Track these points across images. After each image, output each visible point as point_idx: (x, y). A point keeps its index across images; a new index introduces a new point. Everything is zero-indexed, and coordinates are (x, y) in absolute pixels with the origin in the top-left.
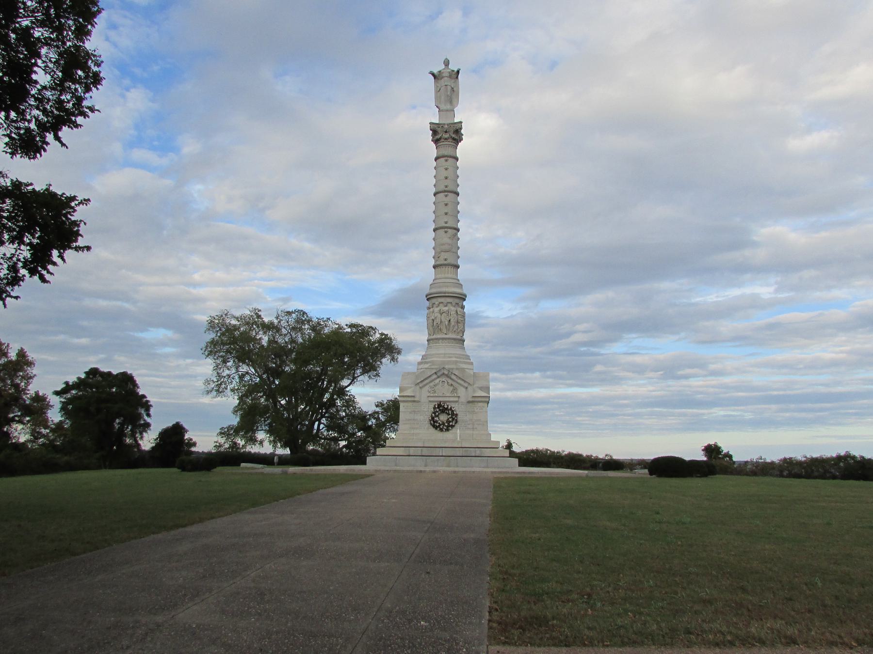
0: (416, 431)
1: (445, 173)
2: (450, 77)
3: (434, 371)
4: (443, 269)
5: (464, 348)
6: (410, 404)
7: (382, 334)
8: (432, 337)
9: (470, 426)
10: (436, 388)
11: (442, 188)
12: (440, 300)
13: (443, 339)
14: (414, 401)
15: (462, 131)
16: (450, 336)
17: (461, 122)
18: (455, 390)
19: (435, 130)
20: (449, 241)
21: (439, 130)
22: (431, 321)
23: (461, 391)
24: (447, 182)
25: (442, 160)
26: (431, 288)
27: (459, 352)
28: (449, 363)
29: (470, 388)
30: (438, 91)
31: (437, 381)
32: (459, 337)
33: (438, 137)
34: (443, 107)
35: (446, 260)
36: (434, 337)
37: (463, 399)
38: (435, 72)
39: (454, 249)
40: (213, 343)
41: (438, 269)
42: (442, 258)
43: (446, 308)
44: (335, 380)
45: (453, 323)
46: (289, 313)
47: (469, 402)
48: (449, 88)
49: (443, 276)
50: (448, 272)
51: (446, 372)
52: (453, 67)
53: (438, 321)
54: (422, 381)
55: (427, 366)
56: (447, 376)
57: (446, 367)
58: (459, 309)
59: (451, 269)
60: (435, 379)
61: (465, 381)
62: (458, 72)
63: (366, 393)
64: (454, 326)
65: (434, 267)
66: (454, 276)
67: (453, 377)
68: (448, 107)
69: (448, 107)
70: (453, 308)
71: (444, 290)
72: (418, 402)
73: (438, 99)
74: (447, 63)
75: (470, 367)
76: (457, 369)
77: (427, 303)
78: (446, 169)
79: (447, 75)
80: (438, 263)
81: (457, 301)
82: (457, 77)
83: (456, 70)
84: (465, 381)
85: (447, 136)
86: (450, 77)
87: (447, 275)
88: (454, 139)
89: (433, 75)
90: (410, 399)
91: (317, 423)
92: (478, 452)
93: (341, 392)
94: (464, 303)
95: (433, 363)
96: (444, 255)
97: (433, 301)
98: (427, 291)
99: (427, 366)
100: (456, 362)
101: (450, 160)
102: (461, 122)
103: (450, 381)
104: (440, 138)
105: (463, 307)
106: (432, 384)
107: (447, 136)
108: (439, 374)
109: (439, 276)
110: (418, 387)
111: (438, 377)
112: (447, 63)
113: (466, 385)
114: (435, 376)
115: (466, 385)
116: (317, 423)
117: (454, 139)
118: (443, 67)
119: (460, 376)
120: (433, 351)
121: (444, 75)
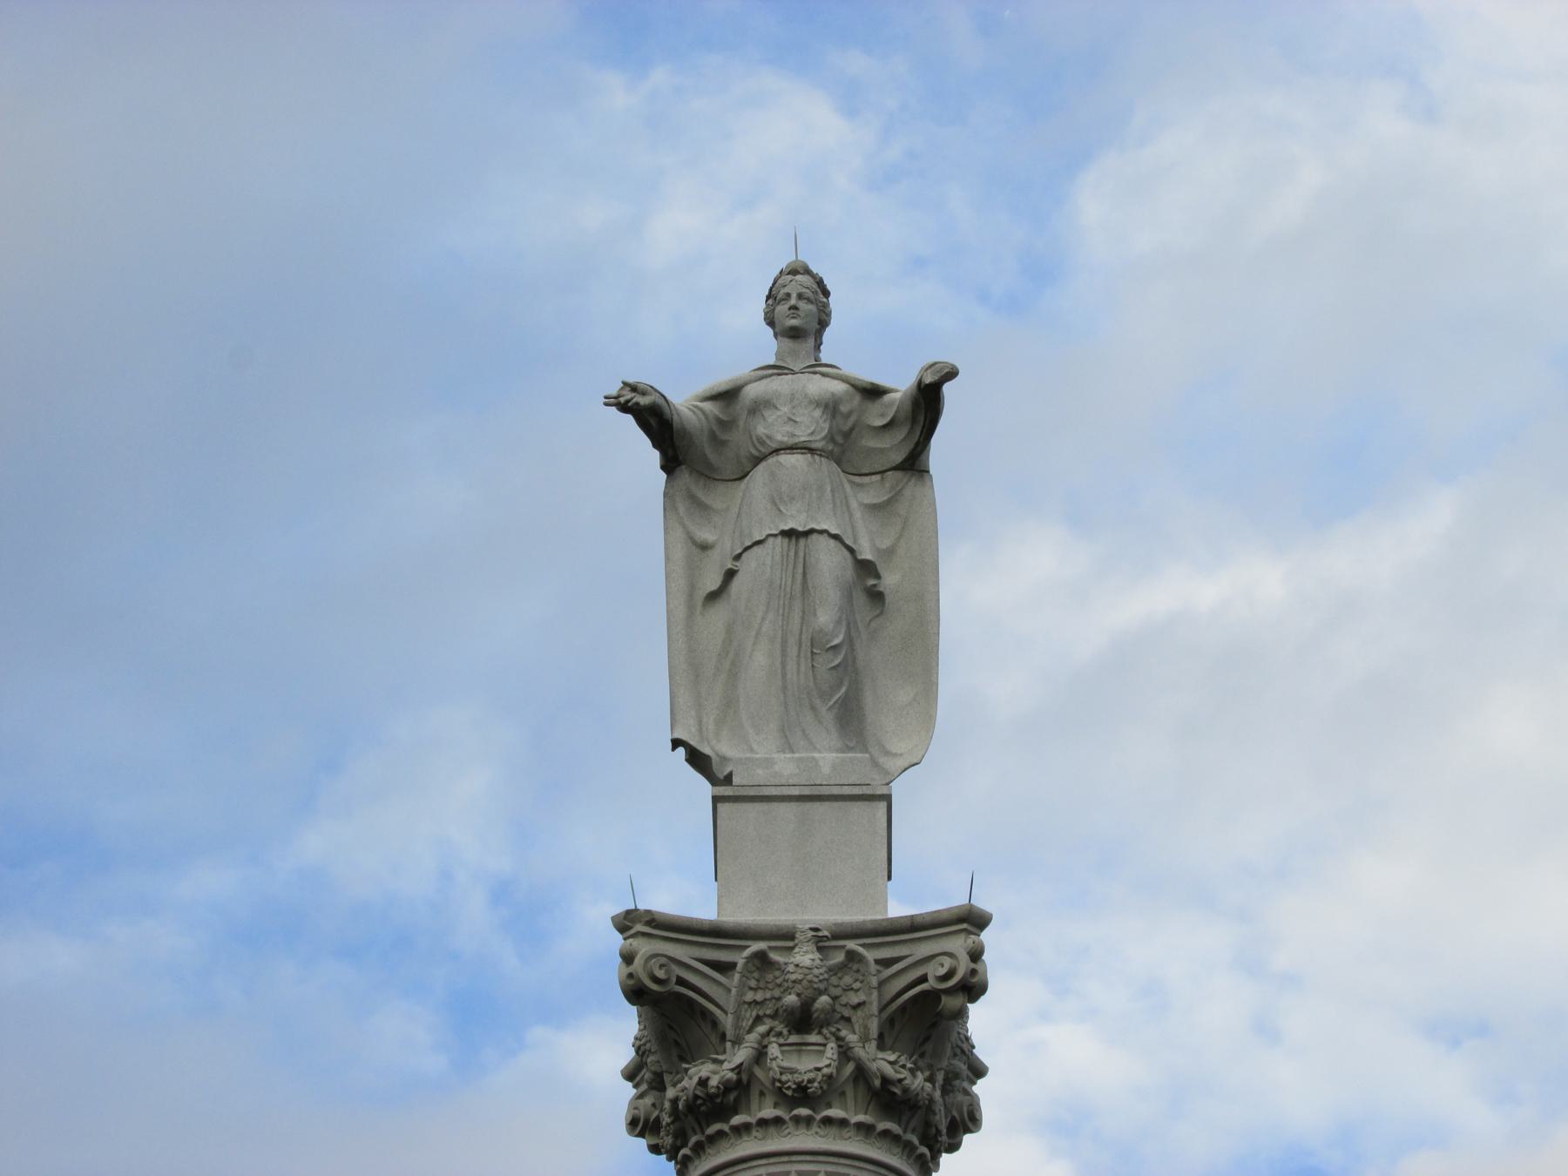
17: (974, 920)
19: (677, 995)
21: (726, 997)
30: (707, 591)
33: (712, 1072)
34: (761, 756)
38: (682, 395)
48: (828, 562)
62: (927, 401)
68: (827, 760)
69: (827, 760)
73: (700, 672)
79: (810, 427)
82: (914, 464)
83: (901, 382)
85: (812, 1062)
88: (888, 1099)
89: (654, 419)
102: (974, 920)
104: (740, 1089)
107: (812, 1062)
112: (799, 309)
117: (888, 1099)
118: (765, 346)
121: (773, 427)
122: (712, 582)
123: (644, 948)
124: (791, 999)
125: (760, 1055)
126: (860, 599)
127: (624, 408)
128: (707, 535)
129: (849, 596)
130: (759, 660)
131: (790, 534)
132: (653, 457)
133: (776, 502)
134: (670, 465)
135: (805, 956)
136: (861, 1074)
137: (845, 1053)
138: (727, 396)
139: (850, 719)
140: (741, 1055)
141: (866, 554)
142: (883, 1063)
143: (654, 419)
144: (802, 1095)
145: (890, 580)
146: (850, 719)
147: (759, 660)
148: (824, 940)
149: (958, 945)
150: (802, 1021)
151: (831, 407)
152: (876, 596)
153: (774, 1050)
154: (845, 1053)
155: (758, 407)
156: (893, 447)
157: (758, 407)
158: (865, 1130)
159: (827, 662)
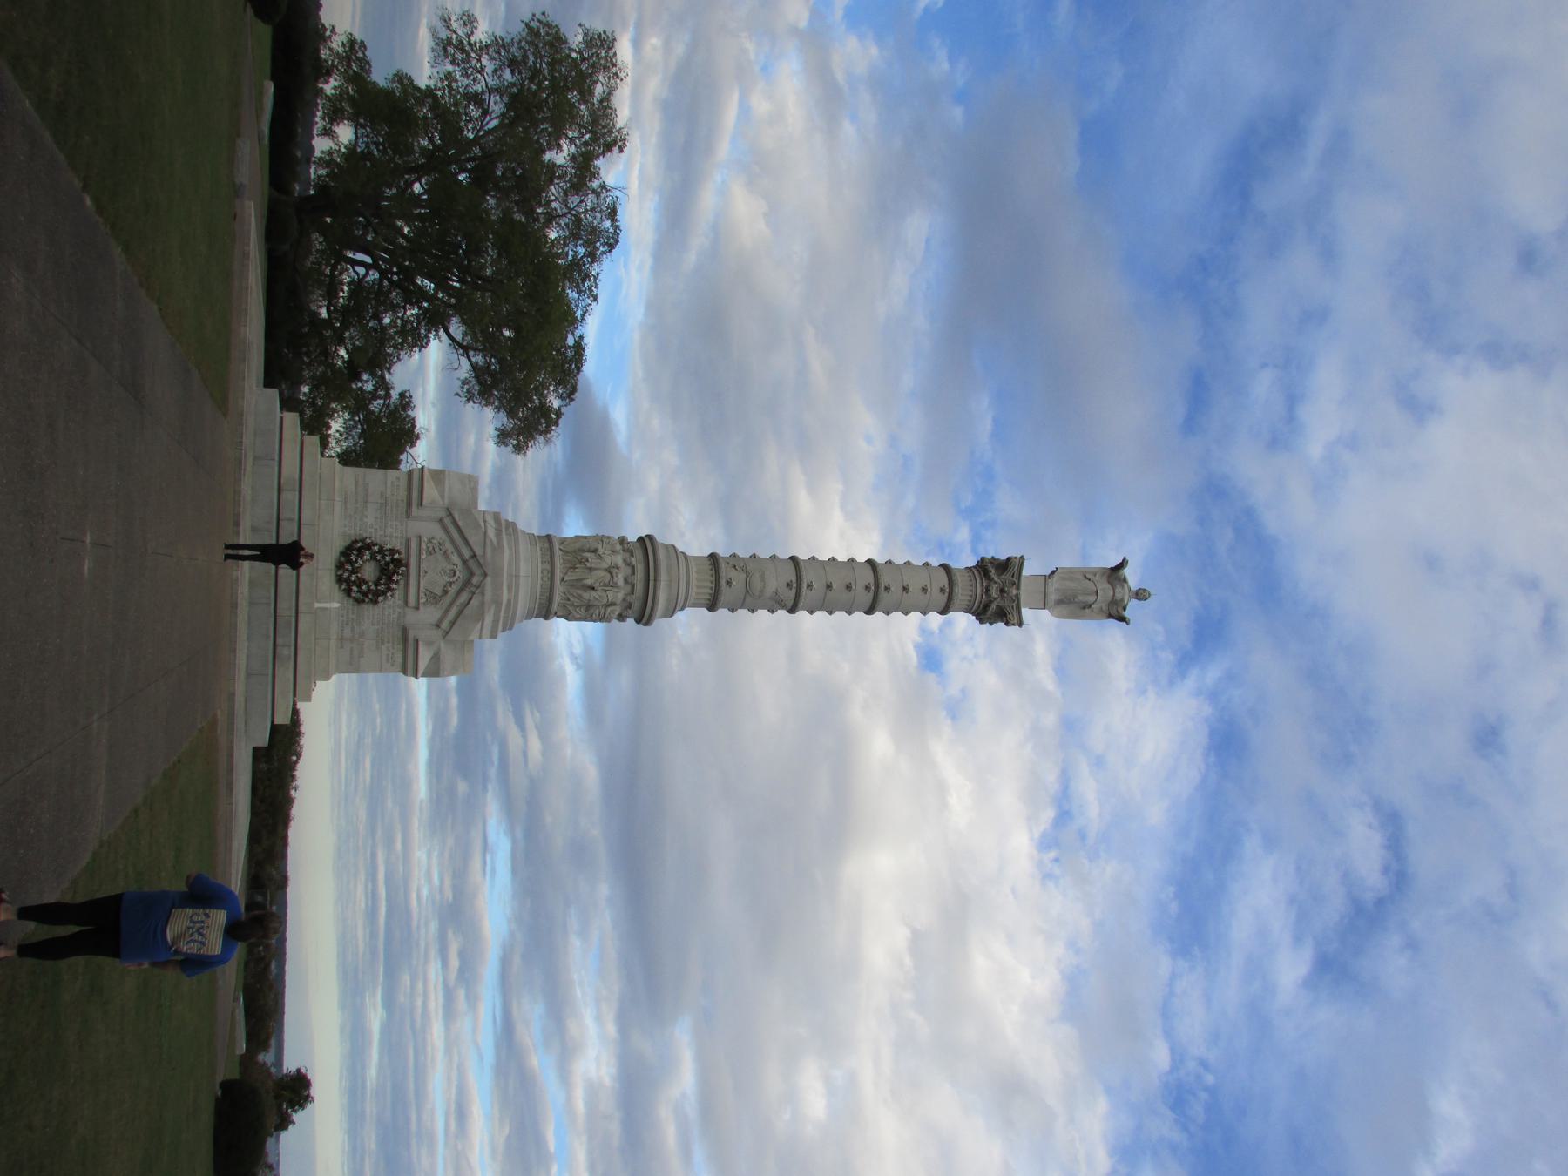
0: (338, 507)
1: (915, 588)
3: (478, 551)
4: (708, 577)
5: (529, 617)
6: (403, 493)
7: (559, 414)
8: (557, 547)
9: (347, 633)
10: (439, 555)
11: (885, 579)
12: (640, 569)
13: (552, 573)
14: (409, 504)
15: (1001, 625)
16: (559, 589)
17: (1020, 624)
18: (434, 599)
19: (1007, 568)
20: (769, 591)
21: (1007, 576)
22: (593, 545)
23: (429, 614)
24: (896, 588)
25: (944, 581)
26: (666, 547)
27: (522, 607)
28: (497, 588)
29: (440, 633)
30: (1086, 575)
31: (455, 559)
32: (555, 607)
33: (993, 573)
34: (1054, 584)
35: (729, 583)
36: (558, 553)
37: (411, 617)
38: (1126, 571)
39: (751, 600)
40: (557, 40)
41: (707, 566)
42: (733, 574)
43: (621, 582)
44: (464, 308)
45: (586, 595)
46: (612, 214)
47: (405, 631)
48: (1091, 599)
49: (694, 575)
50: (700, 584)
51: (475, 580)
52: (1133, 609)
53: (593, 561)
54: (455, 523)
55: (491, 533)
56: (467, 583)
57: (489, 579)
58: (618, 610)
59: (707, 592)
60: (461, 555)
61: (453, 623)
62: (1122, 619)
63: (429, 373)
64: (580, 597)
65: (713, 557)
66: (691, 600)
67: (464, 597)
68: (1053, 597)
69: (1053, 597)
70: (620, 596)
71: (663, 577)
72: (408, 515)
73: (1070, 573)
74: (1141, 595)
75: (487, 630)
76: (483, 603)
77: (632, 538)
78: (924, 590)
79: (1118, 596)
80: (723, 566)
81: (637, 605)
82: (1110, 616)
83: (1126, 614)
84: (453, 623)
85: (994, 593)
87: (694, 583)
89: (1121, 566)
90: (415, 494)
91: (368, 260)
92: (285, 652)
93: (435, 320)
94: (631, 622)
95: (498, 548)
96: (738, 578)
97: (639, 553)
98: (659, 539)
99: (491, 533)
100: (498, 603)
101: (943, 599)
102: (1020, 624)
103: (453, 590)
105: (621, 618)
106: (449, 546)
107: (994, 593)
108: (471, 563)
109: (693, 568)
110: (443, 514)
111: (465, 562)
112: (1141, 595)
113: (445, 625)
114: (467, 553)
115: (445, 625)
116: (368, 260)
117: (986, 607)
119: (467, 611)
120: (524, 548)
121: (1118, 589)
138: (1125, 580)
139: (1060, 602)
142: (993, 606)
143: (1121, 566)
146: (1060, 602)
147: (1072, 585)
148: (1018, 596)
150: (1002, 591)
156: (1114, 612)
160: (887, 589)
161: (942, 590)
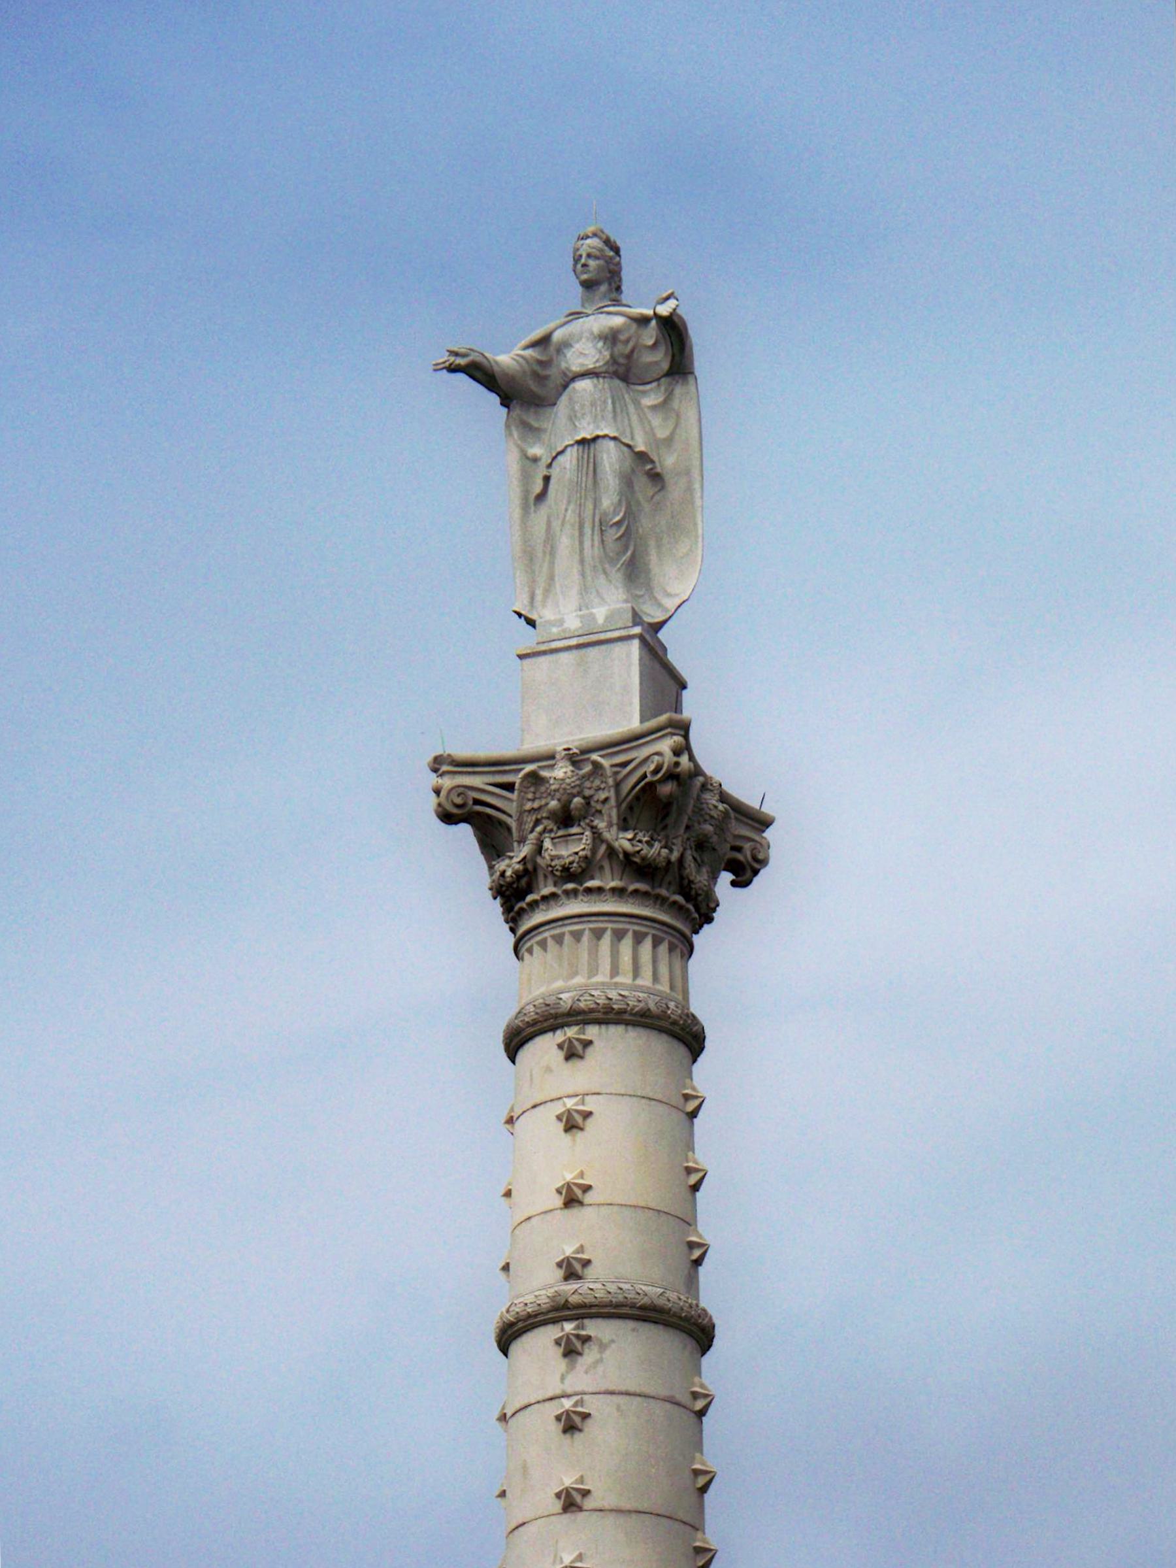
2: (622, 370)
11: (540, 1284)
33: (510, 865)
48: (610, 458)
73: (535, 557)
85: (567, 850)
86: (622, 370)
88: (637, 868)
89: (480, 373)
101: (614, 1049)
107: (567, 850)
117: (637, 868)
122: (538, 488)
123: (447, 783)
124: (554, 804)
125: (539, 849)
126: (641, 482)
127: (453, 369)
128: (536, 450)
129: (627, 482)
130: (565, 543)
131: (582, 442)
132: (494, 399)
133: (572, 418)
134: (506, 402)
135: (561, 771)
136: (611, 852)
137: (597, 836)
139: (635, 571)
140: (525, 850)
141: (641, 447)
142: (623, 841)
143: (480, 373)
144: (567, 874)
145: (668, 461)
146: (635, 571)
147: (565, 543)
148: (575, 759)
149: (665, 746)
150: (565, 819)
151: (611, 338)
152: (656, 477)
153: (547, 844)
154: (597, 836)
155: (566, 344)
157: (566, 344)
158: (619, 892)
159: (613, 534)
160: (572, 1270)
161: (572, 1053)
